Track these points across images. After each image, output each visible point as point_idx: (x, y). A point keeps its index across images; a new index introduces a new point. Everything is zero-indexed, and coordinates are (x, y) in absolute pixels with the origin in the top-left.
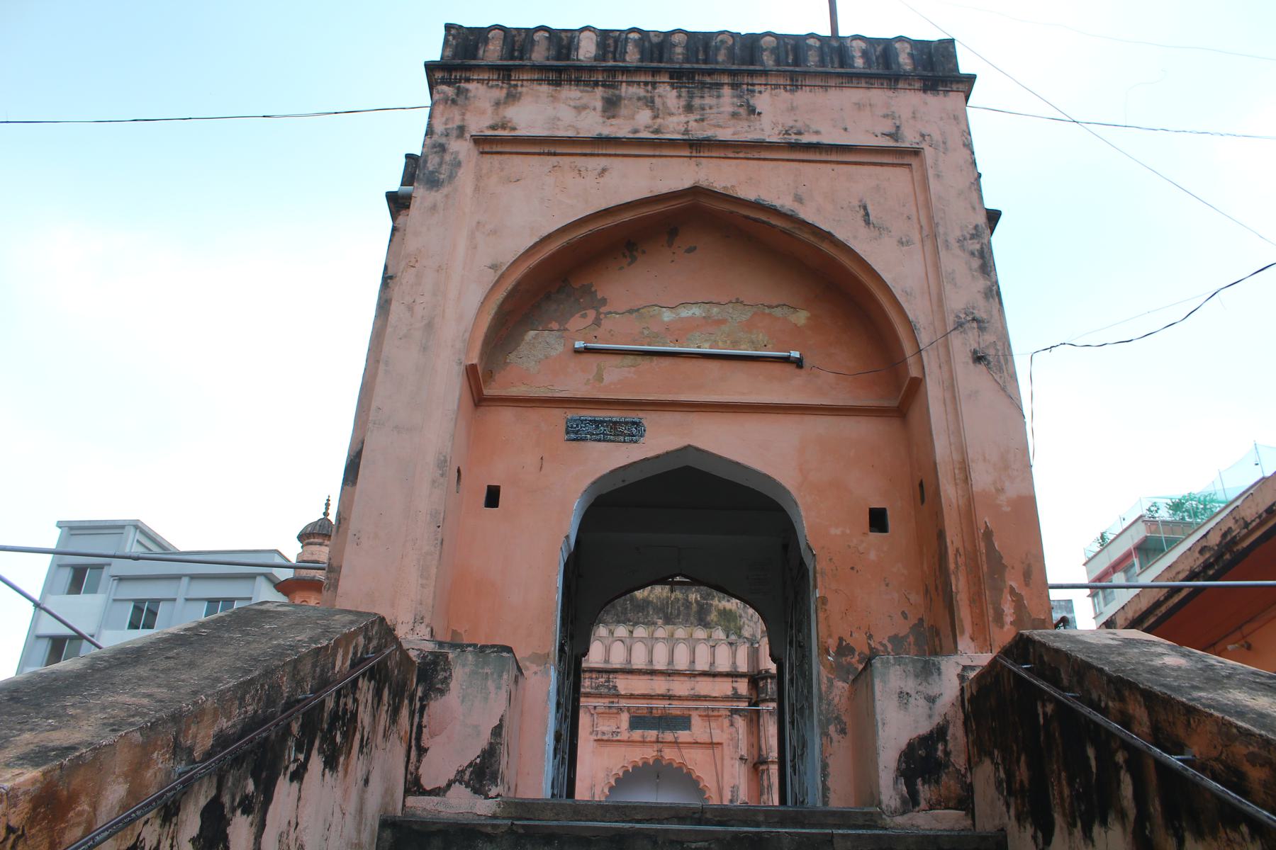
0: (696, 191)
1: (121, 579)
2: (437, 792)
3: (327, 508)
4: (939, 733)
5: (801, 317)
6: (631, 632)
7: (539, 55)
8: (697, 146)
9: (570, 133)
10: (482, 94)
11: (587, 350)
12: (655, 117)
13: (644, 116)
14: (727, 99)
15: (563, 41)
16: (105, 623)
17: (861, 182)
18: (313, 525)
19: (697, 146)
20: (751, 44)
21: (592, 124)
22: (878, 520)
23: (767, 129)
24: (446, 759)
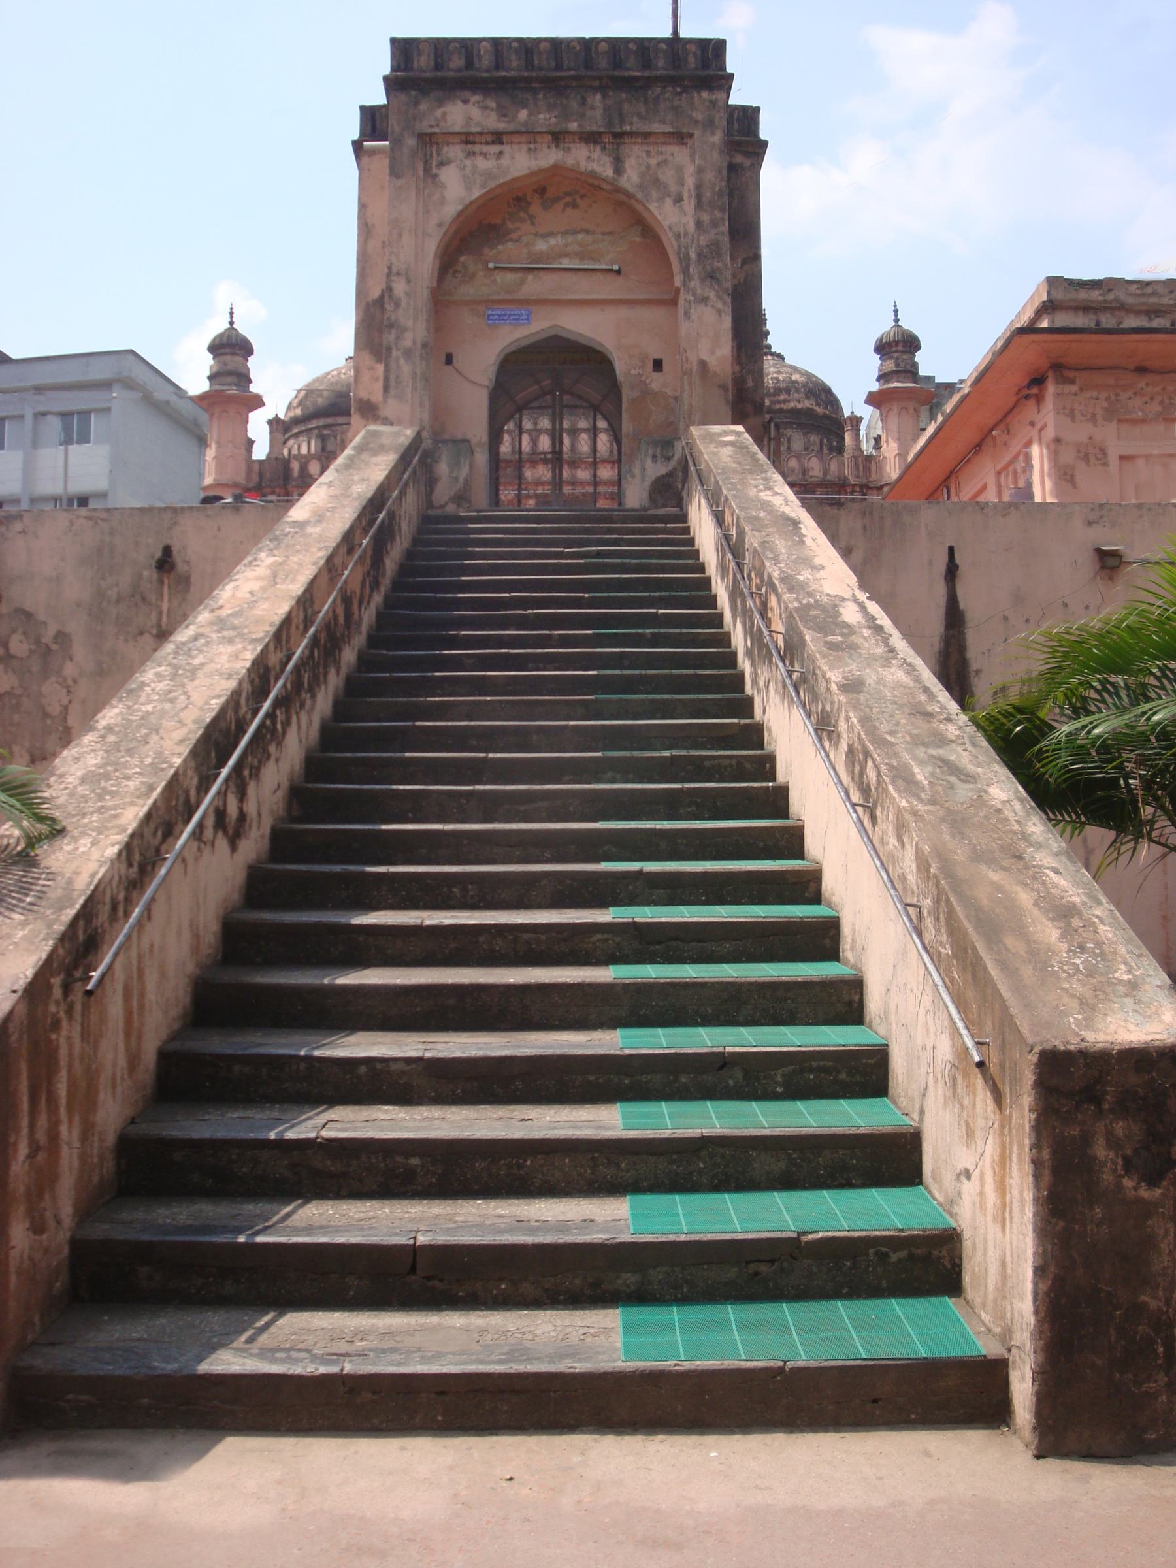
0: (556, 167)
2: (442, 507)
3: (232, 317)
4: (670, 475)
6: (535, 424)
8: (558, 137)
9: (478, 130)
11: (496, 268)
12: (530, 115)
18: (221, 336)
21: (492, 122)
24: (443, 493)
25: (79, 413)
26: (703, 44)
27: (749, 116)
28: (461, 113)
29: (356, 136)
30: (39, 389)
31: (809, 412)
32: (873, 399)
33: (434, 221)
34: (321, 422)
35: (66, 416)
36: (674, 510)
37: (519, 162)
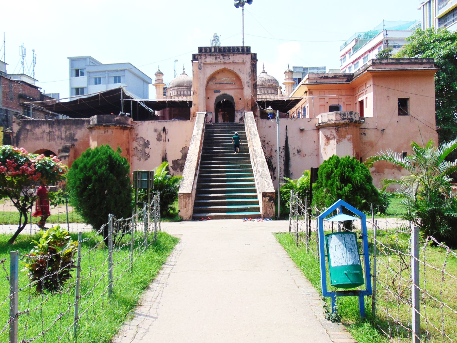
0: (224, 69)
1: (89, 72)
5: (234, 79)
7: (208, 51)
8: (224, 63)
10: (203, 57)
13: (219, 60)
14: (227, 57)
15: (210, 48)
16: (89, 83)
17: (239, 67)
19: (224, 63)
20: (229, 48)
21: (214, 61)
22: (240, 99)
23: (231, 61)
24: (208, 121)
25: (118, 77)
26: (247, 47)
27: (255, 55)
28: (210, 59)
29: (192, 59)
30: (108, 71)
31: (272, 85)
32: (283, 84)
33: (206, 77)
34: (177, 88)
35: (115, 77)
36: (242, 123)
37: (219, 67)
